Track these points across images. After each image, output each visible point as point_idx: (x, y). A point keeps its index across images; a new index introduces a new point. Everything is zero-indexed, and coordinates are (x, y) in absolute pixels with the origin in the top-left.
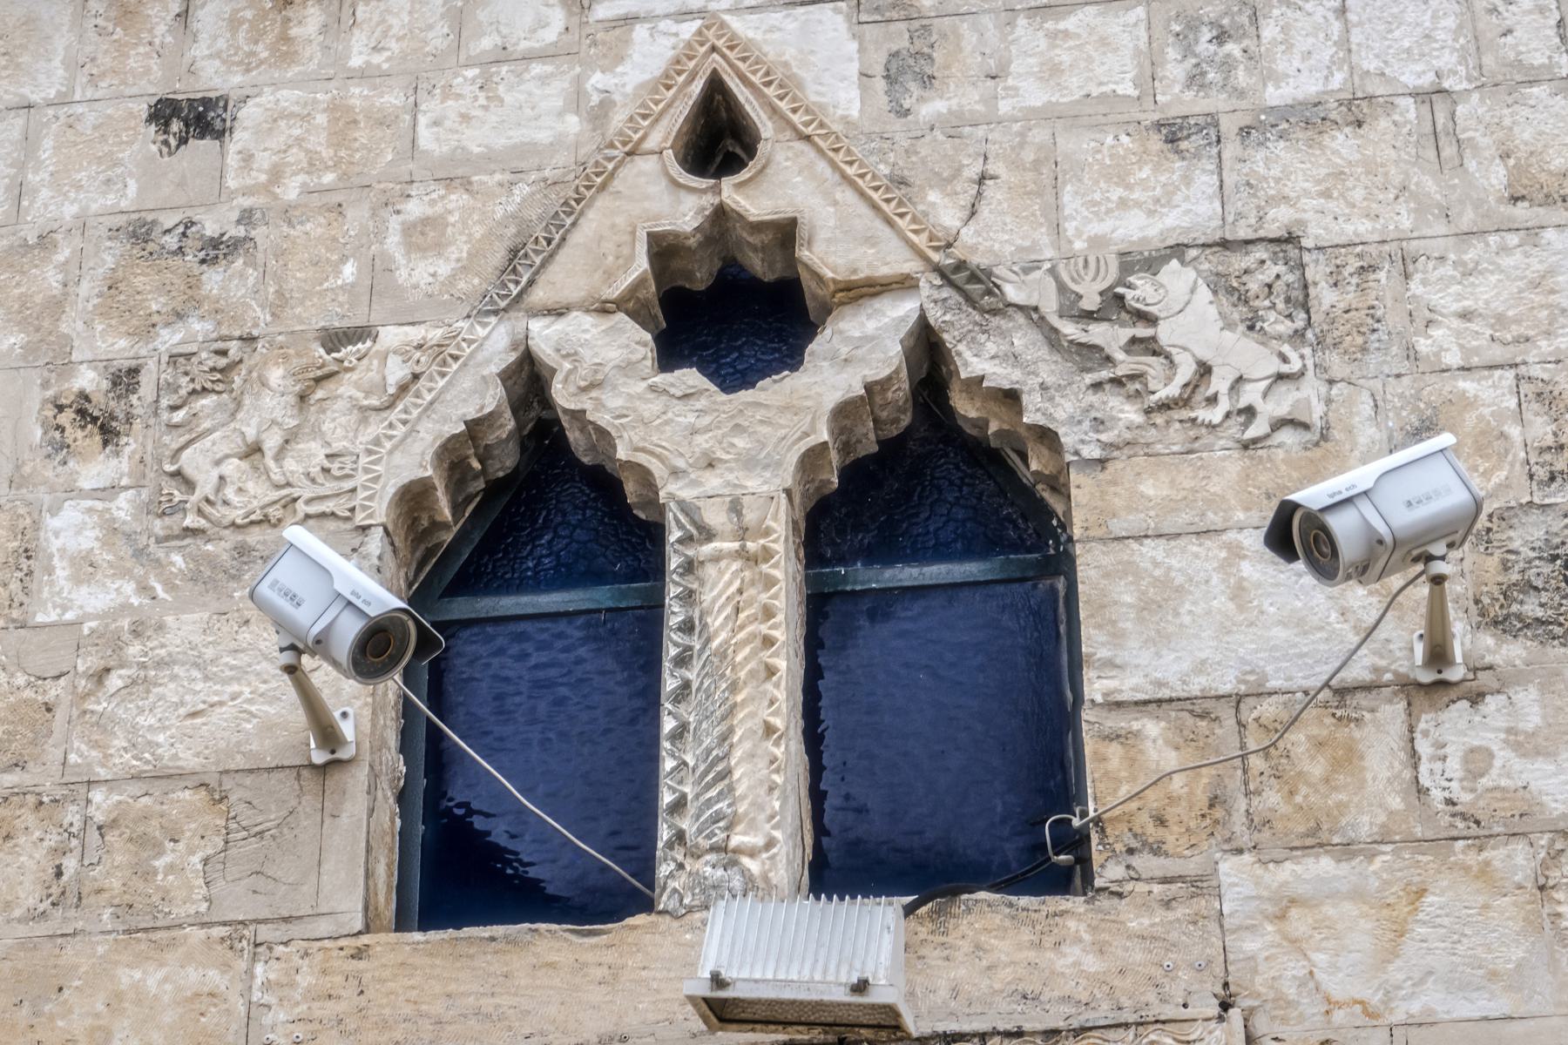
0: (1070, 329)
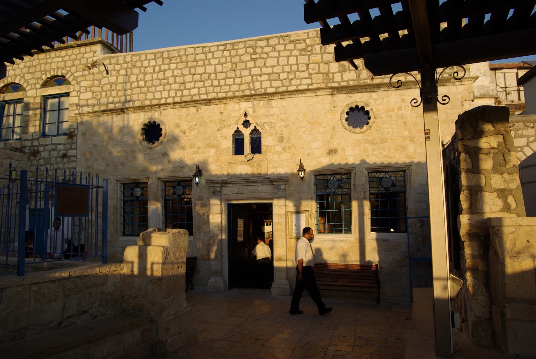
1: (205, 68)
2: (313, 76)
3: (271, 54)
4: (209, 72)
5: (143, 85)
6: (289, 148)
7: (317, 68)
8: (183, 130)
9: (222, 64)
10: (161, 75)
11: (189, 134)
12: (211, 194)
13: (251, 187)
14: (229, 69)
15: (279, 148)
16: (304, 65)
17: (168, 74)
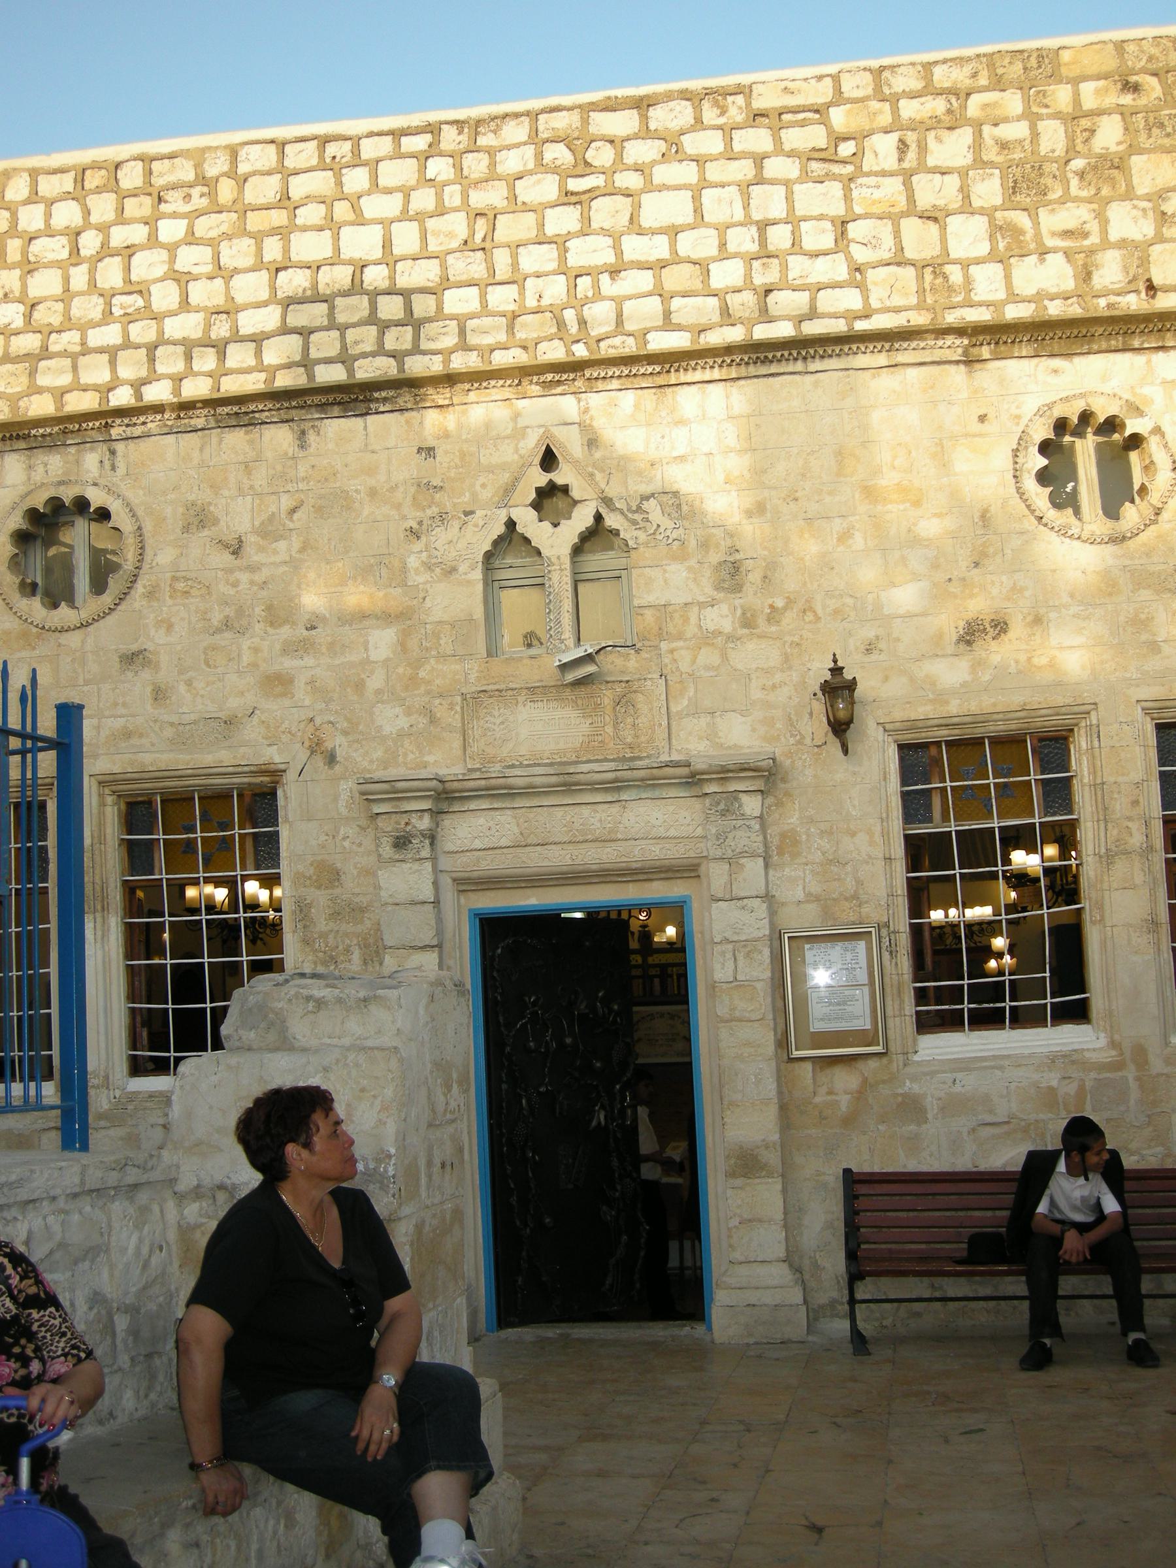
0: (630, 515)
1: (336, 238)
2: (871, 274)
3: (664, 174)
4: (357, 255)
5: (19, 323)
6: (774, 615)
7: (888, 241)
8: (230, 538)
9: (420, 218)
10: (111, 274)
11: (257, 558)
12: (387, 850)
13: (586, 811)
14: (455, 244)
15: (720, 618)
16: (828, 225)
17: (148, 265)
